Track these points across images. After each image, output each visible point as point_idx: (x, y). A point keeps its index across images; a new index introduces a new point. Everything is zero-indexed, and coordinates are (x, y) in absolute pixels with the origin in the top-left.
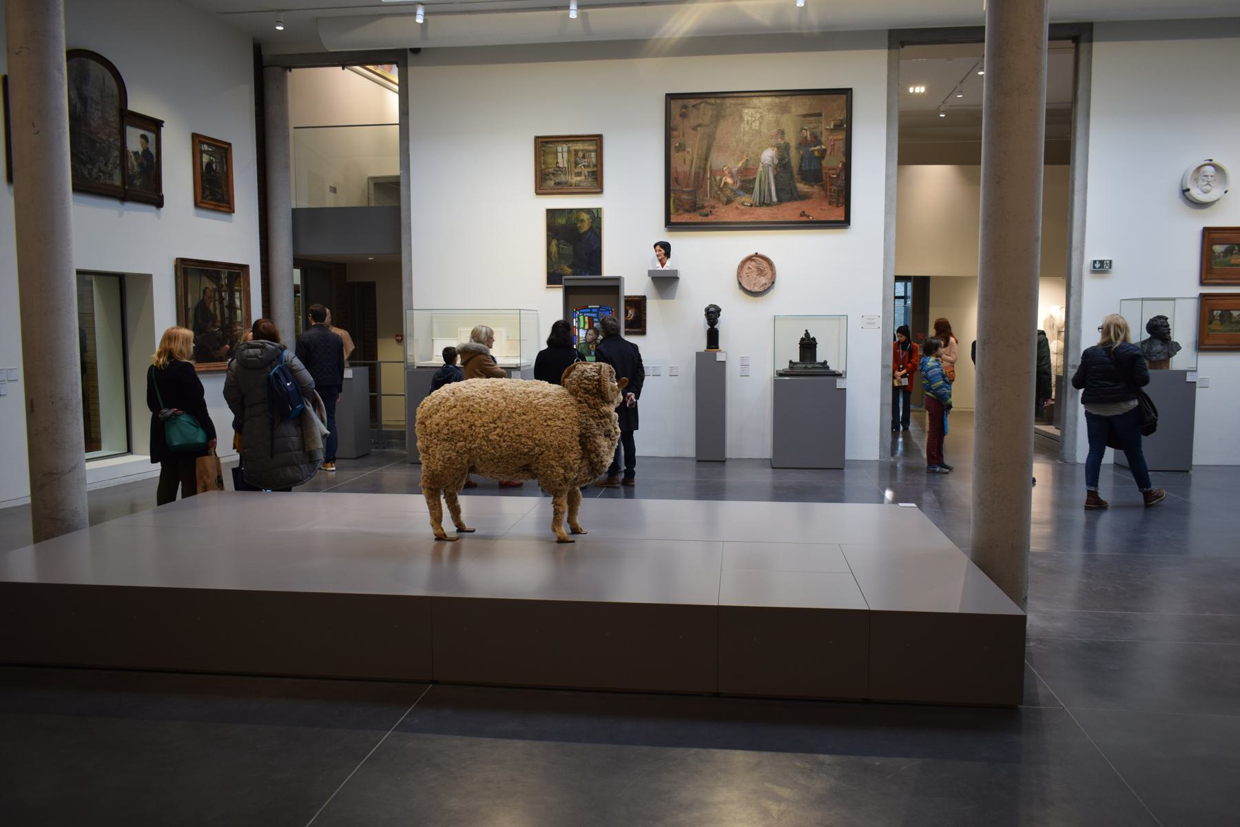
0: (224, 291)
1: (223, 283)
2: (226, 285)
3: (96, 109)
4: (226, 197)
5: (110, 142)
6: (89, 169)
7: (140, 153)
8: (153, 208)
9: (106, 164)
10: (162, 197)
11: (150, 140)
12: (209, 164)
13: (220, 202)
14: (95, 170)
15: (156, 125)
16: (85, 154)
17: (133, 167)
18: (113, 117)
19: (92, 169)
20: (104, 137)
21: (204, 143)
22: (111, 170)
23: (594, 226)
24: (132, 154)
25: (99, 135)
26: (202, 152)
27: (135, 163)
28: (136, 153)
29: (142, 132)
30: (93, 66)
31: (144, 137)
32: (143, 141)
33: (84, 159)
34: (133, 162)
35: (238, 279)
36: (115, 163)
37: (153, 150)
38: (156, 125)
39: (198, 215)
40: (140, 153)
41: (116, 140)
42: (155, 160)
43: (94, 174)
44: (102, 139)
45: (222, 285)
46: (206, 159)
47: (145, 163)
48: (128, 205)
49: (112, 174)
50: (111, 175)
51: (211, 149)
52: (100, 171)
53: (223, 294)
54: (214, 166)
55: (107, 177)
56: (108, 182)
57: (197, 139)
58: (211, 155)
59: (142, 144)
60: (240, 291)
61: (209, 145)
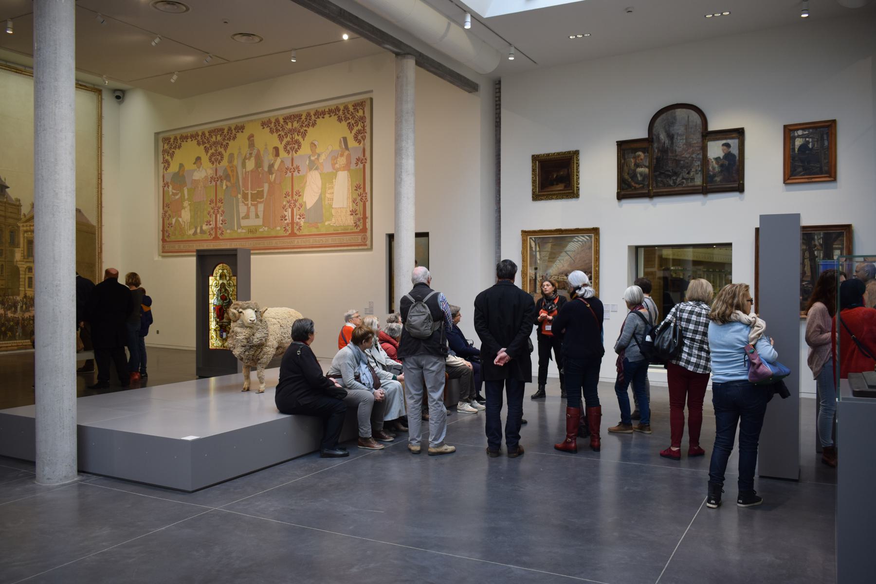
0: (818, 250)
1: (817, 243)
2: (821, 245)
3: (681, 139)
4: (825, 168)
5: (692, 157)
6: (673, 180)
7: (722, 158)
8: (737, 194)
9: (688, 173)
10: (743, 184)
11: (732, 145)
12: (803, 147)
13: (818, 174)
14: (678, 180)
15: (740, 133)
16: (671, 171)
17: (714, 168)
18: (696, 139)
19: (676, 179)
20: (687, 156)
21: (798, 130)
22: (693, 176)
23: (626, 177)
24: (713, 160)
25: (683, 156)
26: (794, 138)
27: (716, 166)
28: (717, 159)
29: (724, 142)
30: (679, 112)
31: (727, 145)
32: (725, 147)
33: (670, 174)
34: (714, 167)
35: (840, 238)
36: (696, 170)
37: (735, 151)
38: (740, 133)
39: (787, 191)
40: (722, 158)
41: (698, 154)
42: (737, 158)
43: (677, 182)
44: (685, 157)
45: (815, 246)
46: (798, 142)
47: (727, 163)
48: (710, 196)
49: (694, 178)
50: (693, 179)
51: (807, 132)
52: (683, 178)
53: (816, 253)
54: (810, 146)
55: (689, 181)
56: (690, 184)
57: (789, 131)
58: (806, 138)
59: (723, 150)
60: (842, 250)
61: (803, 129)
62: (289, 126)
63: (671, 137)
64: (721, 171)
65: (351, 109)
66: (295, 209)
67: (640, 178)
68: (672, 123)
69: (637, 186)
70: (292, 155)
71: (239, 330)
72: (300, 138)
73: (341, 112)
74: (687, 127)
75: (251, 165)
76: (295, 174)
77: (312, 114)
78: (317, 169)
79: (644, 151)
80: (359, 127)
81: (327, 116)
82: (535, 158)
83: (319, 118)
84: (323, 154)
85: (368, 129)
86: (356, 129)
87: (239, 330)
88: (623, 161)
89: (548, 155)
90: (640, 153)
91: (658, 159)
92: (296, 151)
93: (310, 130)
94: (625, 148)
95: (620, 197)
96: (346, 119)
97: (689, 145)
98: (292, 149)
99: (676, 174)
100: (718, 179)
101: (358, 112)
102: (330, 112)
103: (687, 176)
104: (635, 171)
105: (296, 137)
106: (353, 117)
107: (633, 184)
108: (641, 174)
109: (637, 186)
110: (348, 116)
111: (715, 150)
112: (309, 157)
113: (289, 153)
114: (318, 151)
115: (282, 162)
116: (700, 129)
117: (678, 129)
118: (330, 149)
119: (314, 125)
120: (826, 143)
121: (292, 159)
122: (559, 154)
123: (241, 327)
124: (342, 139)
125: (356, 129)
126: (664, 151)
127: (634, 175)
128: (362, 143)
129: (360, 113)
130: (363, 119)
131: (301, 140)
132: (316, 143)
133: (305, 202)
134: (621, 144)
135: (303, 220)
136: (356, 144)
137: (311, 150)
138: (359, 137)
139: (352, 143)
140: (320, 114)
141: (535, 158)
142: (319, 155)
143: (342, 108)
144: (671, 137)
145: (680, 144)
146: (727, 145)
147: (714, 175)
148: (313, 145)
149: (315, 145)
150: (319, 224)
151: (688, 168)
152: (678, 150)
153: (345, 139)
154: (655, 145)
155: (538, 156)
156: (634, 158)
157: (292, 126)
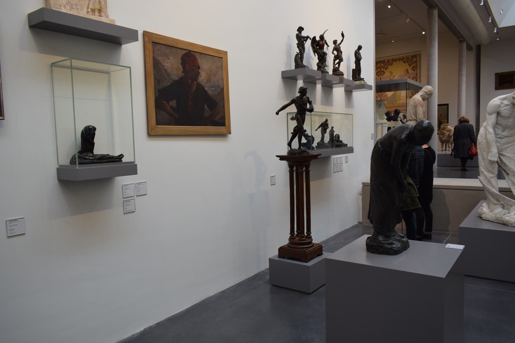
65: (410, 58)
66: (382, 97)
70: (381, 76)
71: (445, 132)
72: (384, 70)
73: (405, 60)
77: (390, 60)
80: (414, 65)
81: (398, 61)
82: (496, 74)
83: (394, 62)
84: (396, 76)
85: (418, 65)
86: (412, 66)
87: (445, 132)
89: (503, 73)
92: (382, 75)
93: (390, 67)
96: (408, 62)
98: (380, 74)
101: (413, 59)
102: (400, 59)
105: (383, 70)
106: (411, 61)
110: (409, 61)
112: (389, 77)
113: (379, 76)
114: (393, 75)
118: (400, 73)
119: (391, 64)
121: (381, 78)
122: (508, 72)
123: (446, 131)
124: (406, 70)
125: (412, 66)
128: (416, 70)
129: (415, 59)
130: (416, 62)
131: (385, 71)
132: (393, 72)
133: (387, 95)
135: (386, 101)
136: (413, 72)
137: (390, 74)
138: (414, 69)
139: (410, 71)
140: (393, 60)
141: (496, 74)
142: (394, 76)
143: (406, 58)
148: (391, 73)
149: (392, 73)
150: (394, 103)
153: (407, 70)
155: (498, 73)
157: (380, 65)
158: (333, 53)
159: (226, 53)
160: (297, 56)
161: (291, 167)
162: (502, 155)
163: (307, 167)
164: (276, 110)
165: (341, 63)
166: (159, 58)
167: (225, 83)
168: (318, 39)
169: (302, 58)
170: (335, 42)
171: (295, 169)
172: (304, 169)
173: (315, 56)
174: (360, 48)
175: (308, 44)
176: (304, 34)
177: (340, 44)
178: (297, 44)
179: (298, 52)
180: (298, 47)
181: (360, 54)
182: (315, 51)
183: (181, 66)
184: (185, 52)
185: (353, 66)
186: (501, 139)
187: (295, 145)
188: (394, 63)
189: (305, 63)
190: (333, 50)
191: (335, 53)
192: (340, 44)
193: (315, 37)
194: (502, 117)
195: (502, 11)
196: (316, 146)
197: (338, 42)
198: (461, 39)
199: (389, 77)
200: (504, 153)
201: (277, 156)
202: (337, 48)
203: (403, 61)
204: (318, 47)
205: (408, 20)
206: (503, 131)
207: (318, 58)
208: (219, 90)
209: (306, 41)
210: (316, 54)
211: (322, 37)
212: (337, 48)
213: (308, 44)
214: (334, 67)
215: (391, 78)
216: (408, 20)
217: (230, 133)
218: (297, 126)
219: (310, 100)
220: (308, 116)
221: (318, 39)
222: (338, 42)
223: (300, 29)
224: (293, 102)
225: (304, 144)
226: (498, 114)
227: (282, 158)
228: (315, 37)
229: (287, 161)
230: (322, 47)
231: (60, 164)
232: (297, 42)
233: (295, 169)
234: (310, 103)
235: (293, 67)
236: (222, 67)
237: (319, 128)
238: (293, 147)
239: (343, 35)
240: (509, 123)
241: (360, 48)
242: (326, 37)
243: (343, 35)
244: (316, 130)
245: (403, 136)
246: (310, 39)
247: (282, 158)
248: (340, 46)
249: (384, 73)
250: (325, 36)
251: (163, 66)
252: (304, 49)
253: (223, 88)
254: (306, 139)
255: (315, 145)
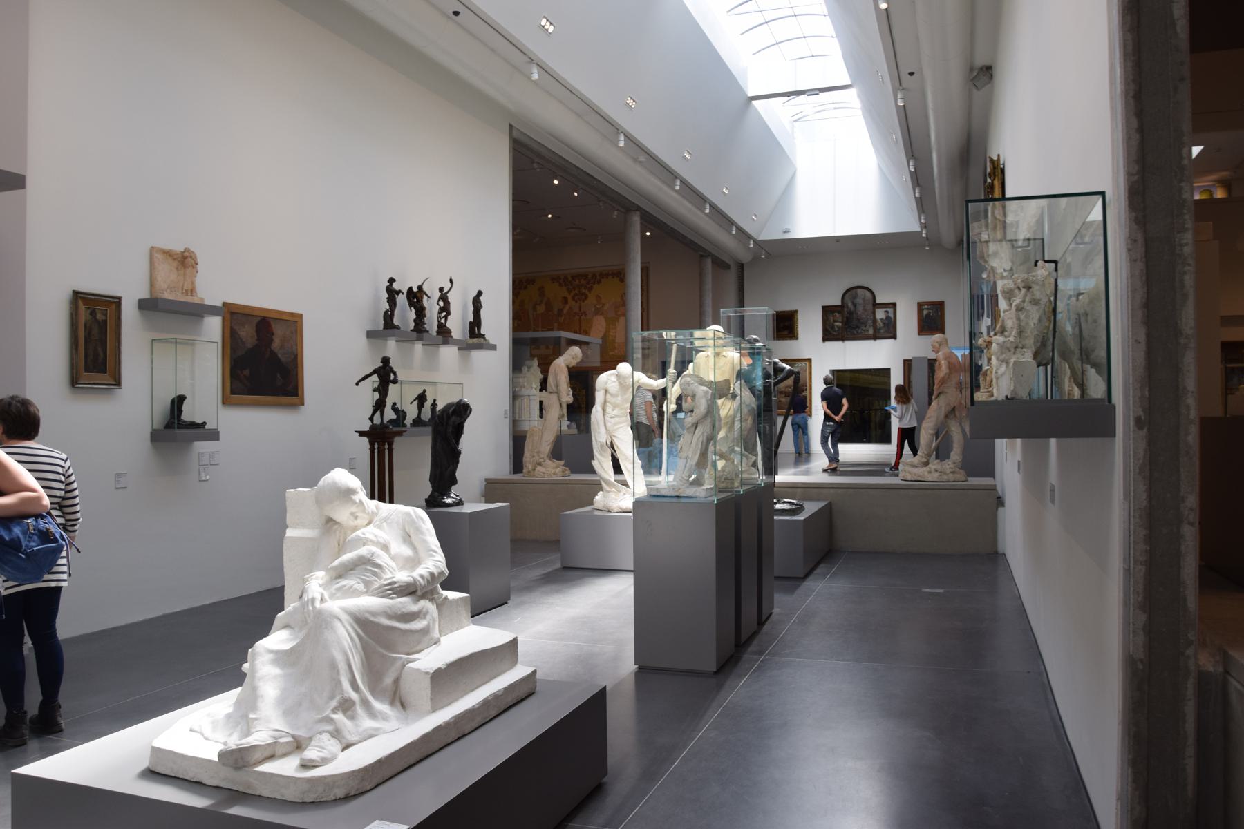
8: (893, 340)
12: (928, 315)
15: (894, 305)
18: (870, 307)
20: (864, 316)
26: (923, 310)
28: (882, 319)
29: (885, 310)
30: (860, 291)
31: (887, 312)
34: (880, 324)
37: (891, 315)
38: (894, 305)
46: (925, 312)
47: (887, 322)
50: (868, 330)
57: (920, 306)
61: (928, 305)
62: (577, 282)
63: (855, 305)
64: (884, 327)
67: (836, 329)
68: (855, 296)
69: (835, 333)
72: (587, 292)
74: (864, 300)
75: (541, 309)
76: (583, 317)
78: (602, 314)
79: (839, 312)
81: (610, 277)
83: (603, 278)
88: (825, 318)
90: (836, 314)
91: (847, 318)
92: (583, 301)
94: (827, 311)
95: (825, 340)
97: (865, 310)
99: (858, 327)
100: (882, 331)
103: (864, 328)
104: (833, 325)
105: (584, 291)
107: (832, 332)
108: (837, 326)
109: (835, 333)
111: (880, 314)
112: (595, 306)
113: (576, 302)
115: (570, 308)
116: (871, 302)
117: (859, 301)
119: (599, 282)
120: (939, 313)
126: (850, 313)
127: (833, 327)
131: (587, 292)
132: (601, 296)
134: (824, 308)
142: (604, 305)
144: (855, 305)
145: (860, 309)
146: (887, 312)
147: (880, 329)
151: (865, 324)
152: (859, 313)
154: (846, 309)
156: (833, 316)
158: (438, 304)
159: (301, 316)
160: (386, 312)
161: (372, 444)
162: (614, 436)
163: (390, 444)
164: (356, 381)
165: (449, 317)
166: (235, 327)
167: (299, 350)
168: (415, 289)
169: (392, 316)
170: (441, 290)
171: (376, 446)
172: (386, 446)
173: (411, 310)
174: (480, 293)
175: (402, 300)
176: (396, 286)
177: (448, 292)
178: (387, 298)
179: (388, 308)
180: (388, 302)
181: (480, 302)
182: (411, 305)
183: (255, 334)
184: (259, 319)
185: (471, 318)
186: (612, 419)
187: (377, 420)
188: (602, 280)
189: (396, 322)
190: (439, 300)
191: (442, 304)
192: (448, 292)
193: (411, 288)
194: (611, 395)
195: (756, 216)
196: (411, 424)
197: (445, 291)
198: (702, 253)
199: (595, 306)
200: (616, 435)
201: (356, 432)
202: (444, 297)
203: (618, 279)
204: (415, 300)
205: (616, 213)
206: (613, 410)
207: (415, 313)
208: (293, 357)
209: (398, 294)
210: (412, 308)
211: (420, 288)
212: (444, 297)
213: (402, 300)
214: (439, 321)
215: (598, 307)
216: (616, 213)
217: (303, 404)
218: (378, 399)
219: (395, 370)
220: (393, 389)
221: (415, 289)
222: (445, 291)
223: (392, 281)
224: (374, 372)
225: (391, 421)
226: (606, 391)
227: (362, 434)
228: (411, 288)
229: (368, 437)
230: (420, 301)
231: (154, 428)
232: (387, 296)
233: (376, 446)
234: (395, 373)
235: (381, 327)
236: (296, 331)
237: (415, 400)
238: (375, 422)
239: (451, 281)
240: (618, 402)
241: (480, 293)
242: (425, 288)
243: (451, 281)
244: (411, 403)
245: (451, 411)
246: (403, 293)
247: (362, 434)
248: (448, 295)
249: (586, 297)
250: (423, 287)
251: (239, 335)
252: (395, 304)
253: (297, 355)
254: (396, 414)
255: (408, 421)
